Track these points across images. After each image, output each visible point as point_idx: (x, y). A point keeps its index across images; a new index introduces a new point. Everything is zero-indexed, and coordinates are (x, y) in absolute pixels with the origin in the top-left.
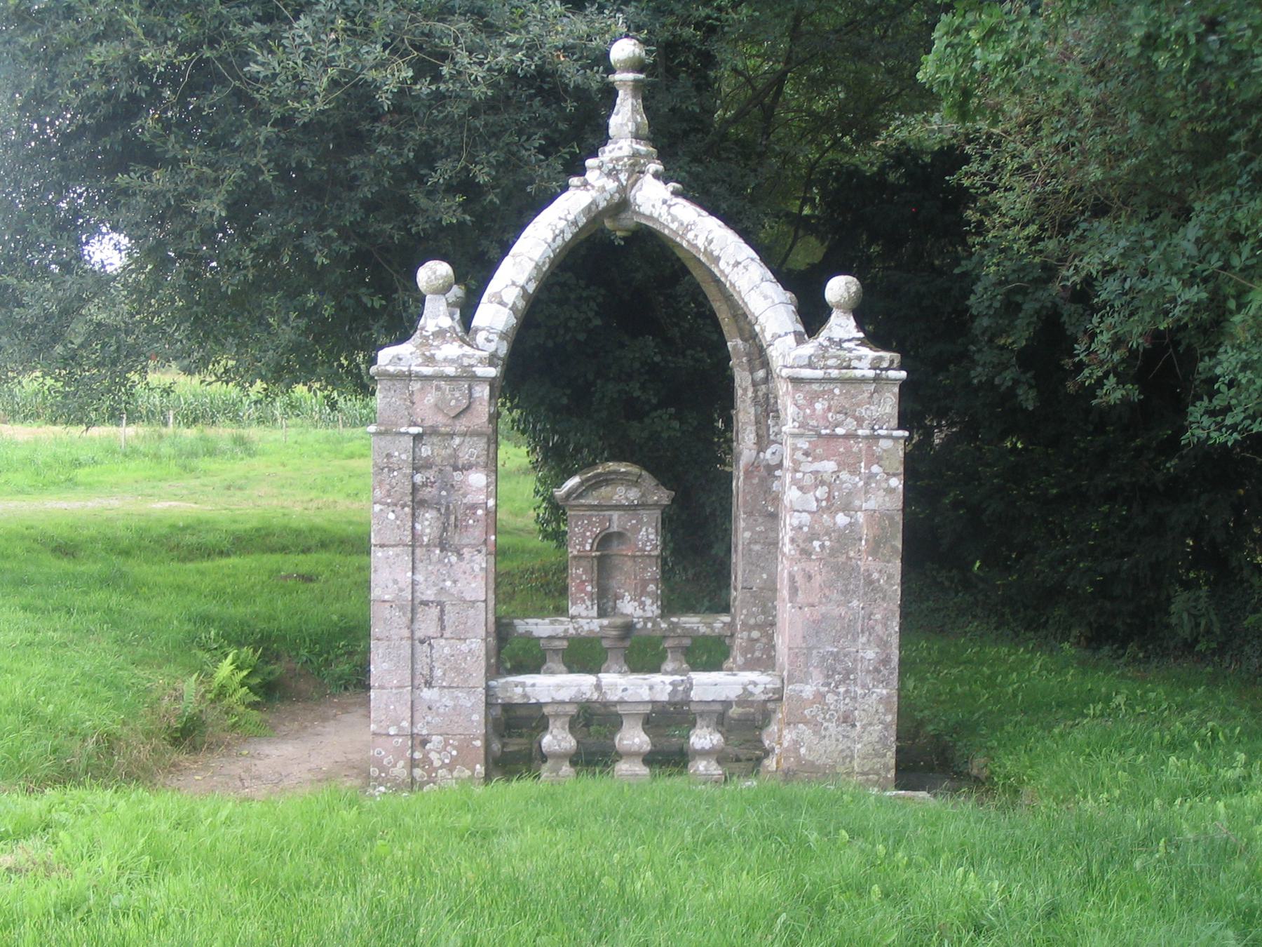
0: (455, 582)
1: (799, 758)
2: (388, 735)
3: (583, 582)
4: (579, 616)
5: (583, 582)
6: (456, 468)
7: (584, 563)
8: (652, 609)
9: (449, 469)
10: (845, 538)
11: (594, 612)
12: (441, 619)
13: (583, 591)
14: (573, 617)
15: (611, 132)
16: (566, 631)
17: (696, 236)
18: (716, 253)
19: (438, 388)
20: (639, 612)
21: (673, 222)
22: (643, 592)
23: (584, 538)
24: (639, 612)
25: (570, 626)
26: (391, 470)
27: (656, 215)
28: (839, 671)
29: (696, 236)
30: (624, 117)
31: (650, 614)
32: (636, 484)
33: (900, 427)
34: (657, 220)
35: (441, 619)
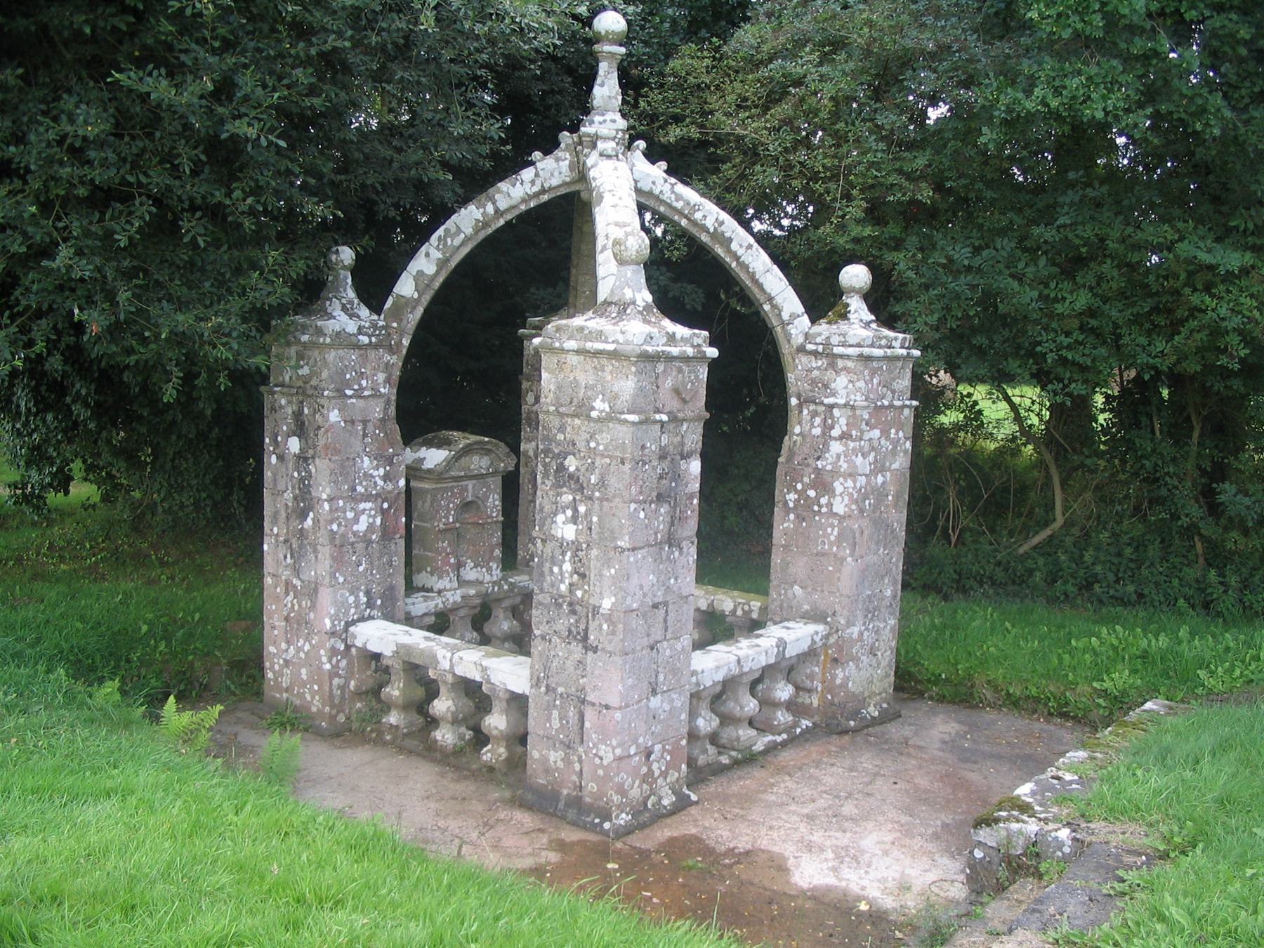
0: (676, 579)
1: (847, 692)
2: (629, 756)
3: (448, 554)
4: (445, 590)
5: (448, 554)
6: (683, 457)
7: (448, 535)
8: (497, 573)
9: (678, 457)
10: (880, 494)
11: (456, 584)
12: (665, 621)
13: (448, 563)
14: (439, 592)
15: (596, 103)
16: (436, 605)
17: (705, 217)
18: (727, 235)
19: (680, 371)
20: (488, 578)
21: (677, 200)
22: (491, 558)
23: (448, 510)
24: (488, 578)
25: (439, 601)
26: (644, 463)
27: (656, 192)
28: (871, 612)
29: (705, 217)
30: (607, 89)
31: (495, 578)
32: (488, 452)
33: (912, 398)
34: (657, 198)
35: (665, 621)
